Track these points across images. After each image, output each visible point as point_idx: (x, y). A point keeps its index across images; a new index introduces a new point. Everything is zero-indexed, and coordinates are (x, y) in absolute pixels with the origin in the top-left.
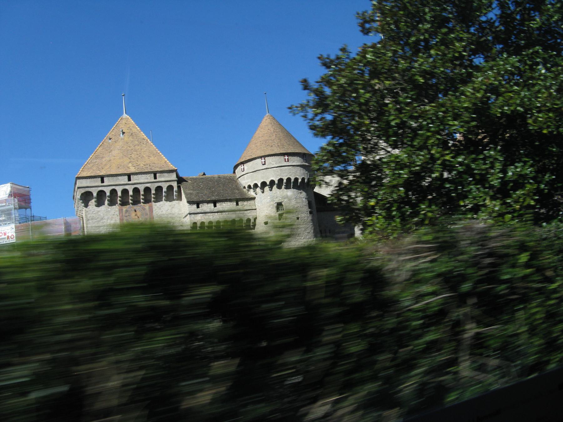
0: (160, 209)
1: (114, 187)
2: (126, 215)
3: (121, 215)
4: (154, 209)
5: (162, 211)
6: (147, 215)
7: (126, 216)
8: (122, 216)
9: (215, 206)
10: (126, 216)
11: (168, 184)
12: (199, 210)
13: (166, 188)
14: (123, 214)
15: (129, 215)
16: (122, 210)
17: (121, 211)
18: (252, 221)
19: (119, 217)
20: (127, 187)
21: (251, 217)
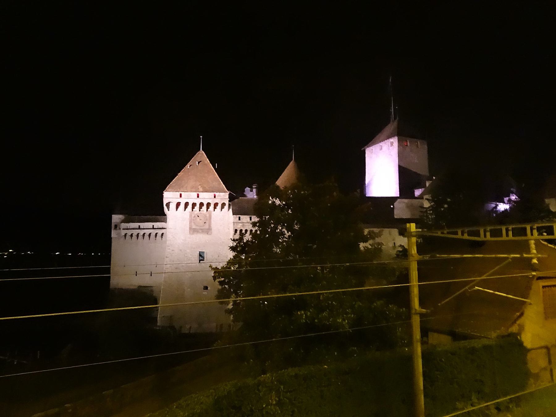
8: (192, 219)
16: (192, 215)
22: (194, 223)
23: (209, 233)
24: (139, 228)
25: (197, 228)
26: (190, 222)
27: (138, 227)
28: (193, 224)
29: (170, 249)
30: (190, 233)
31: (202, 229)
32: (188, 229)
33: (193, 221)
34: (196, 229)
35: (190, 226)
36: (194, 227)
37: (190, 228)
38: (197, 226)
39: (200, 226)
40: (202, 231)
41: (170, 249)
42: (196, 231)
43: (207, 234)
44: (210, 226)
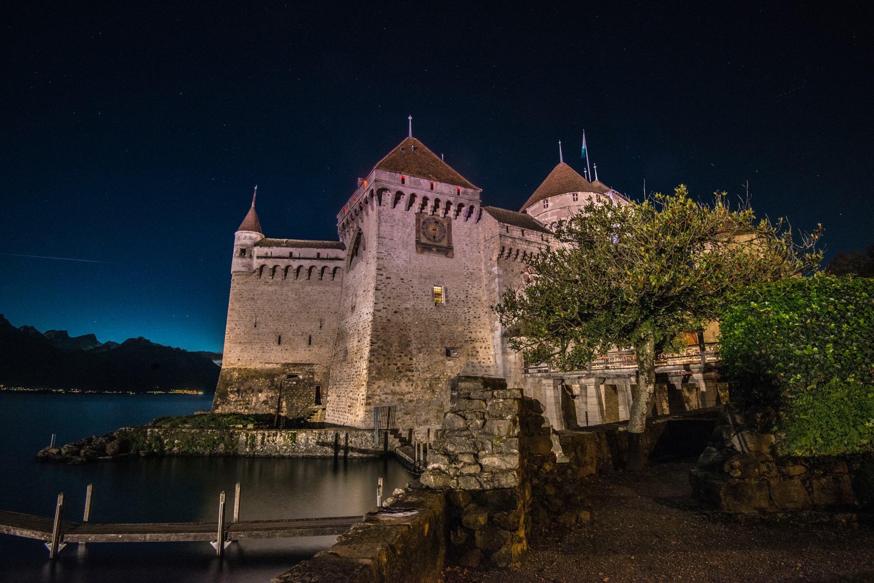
0: (459, 229)
4: (452, 228)
5: (461, 232)
8: (419, 227)
10: (424, 229)
12: (508, 235)
14: (419, 225)
16: (419, 220)
19: (415, 227)
20: (429, 195)
22: (424, 233)
23: (449, 255)
24: (291, 256)
25: (429, 242)
26: (418, 231)
28: (422, 235)
29: (382, 275)
31: (437, 247)
32: (414, 242)
33: (422, 230)
34: (427, 245)
36: (424, 240)
37: (418, 242)
40: (437, 250)
41: (382, 275)
42: (427, 248)
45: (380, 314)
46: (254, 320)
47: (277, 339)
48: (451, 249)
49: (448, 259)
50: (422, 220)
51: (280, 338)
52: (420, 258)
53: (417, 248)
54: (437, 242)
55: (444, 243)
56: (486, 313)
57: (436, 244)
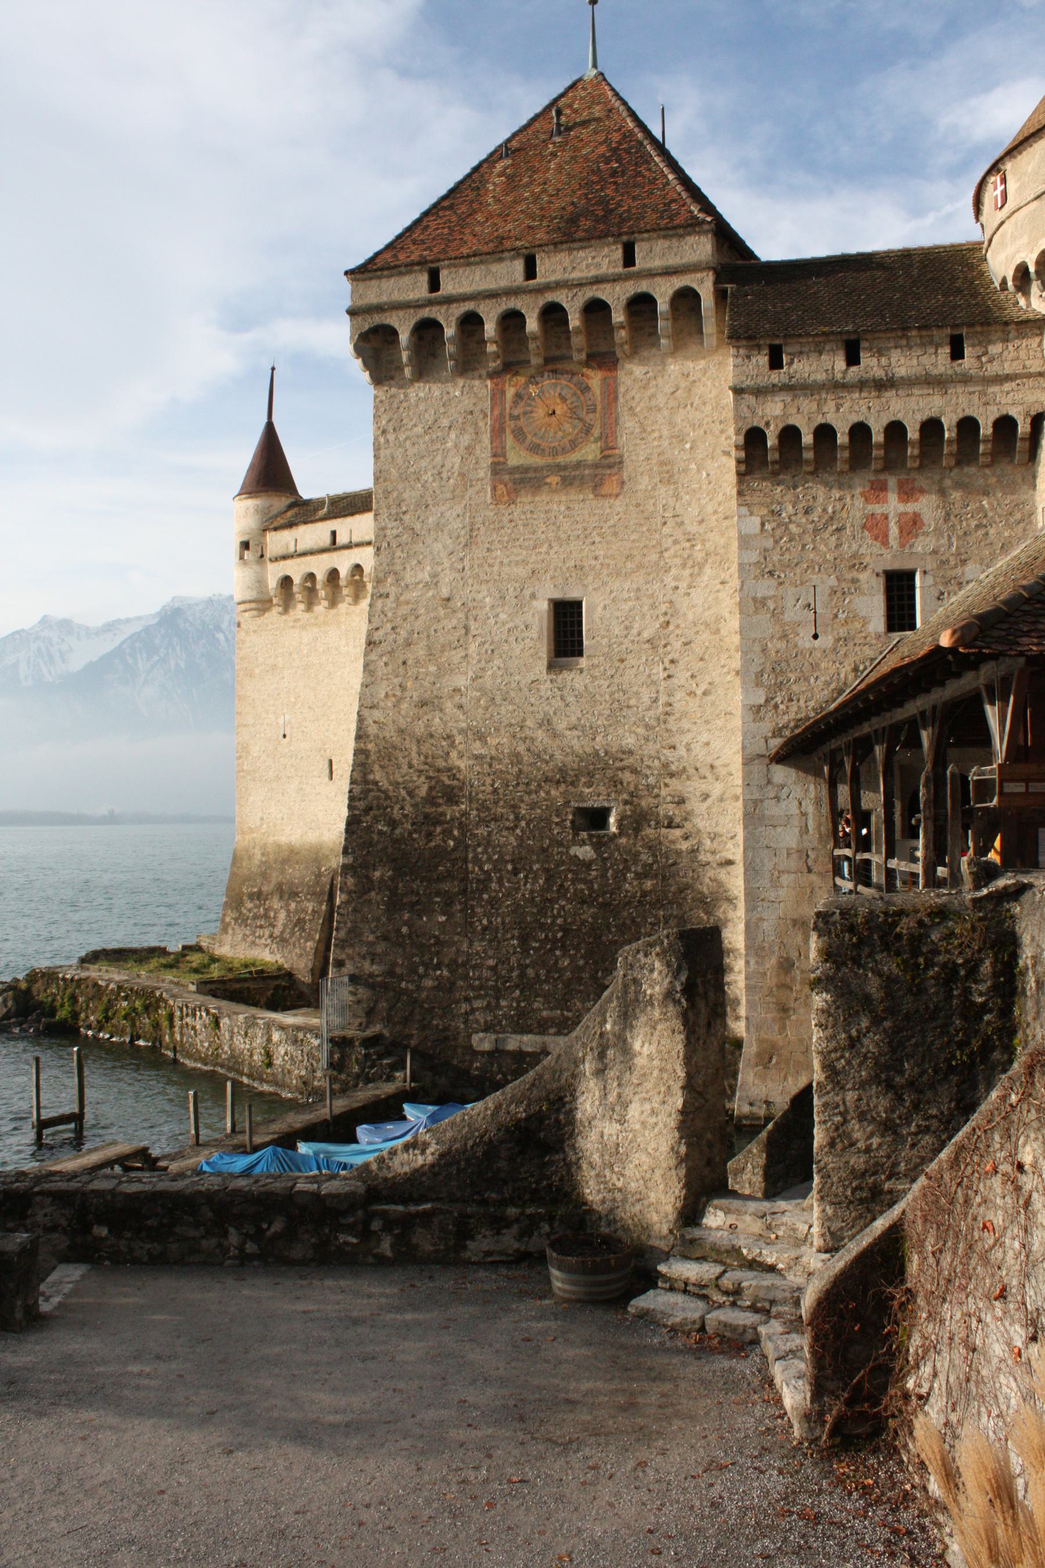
1: (468, 306)
2: (516, 413)
3: (497, 412)
4: (622, 389)
6: (594, 411)
7: (517, 418)
9: (853, 360)
11: (679, 282)
12: (776, 377)
13: (667, 299)
14: (504, 409)
15: (525, 413)
16: (503, 393)
17: (497, 396)
18: (1023, 428)
21: (1014, 412)
22: (519, 435)
24: (334, 546)
26: (498, 432)
27: (327, 541)
28: (509, 440)
30: (494, 496)
31: (565, 468)
32: (483, 472)
33: (510, 425)
34: (526, 469)
35: (494, 455)
36: (517, 457)
37: (497, 469)
38: (535, 449)
39: (554, 452)
40: (564, 479)
43: (595, 488)
44: (608, 445)
45: (377, 714)
46: (281, 721)
47: (327, 766)
48: (610, 467)
49: (601, 502)
50: (510, 392)
51: (331, 761)
52: (505, 519)
53: (494, 489)
54: (564, 451)
55: (590, 452)
56: (737, 673)
57: (560, 459)
